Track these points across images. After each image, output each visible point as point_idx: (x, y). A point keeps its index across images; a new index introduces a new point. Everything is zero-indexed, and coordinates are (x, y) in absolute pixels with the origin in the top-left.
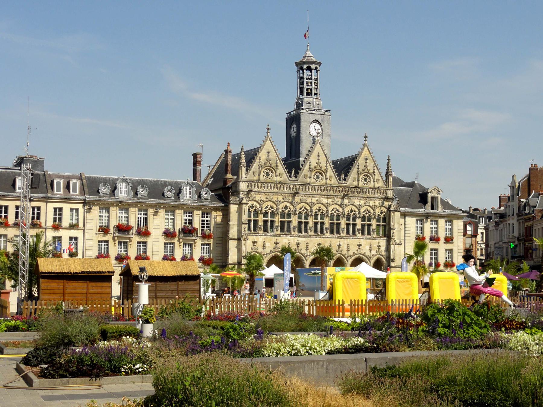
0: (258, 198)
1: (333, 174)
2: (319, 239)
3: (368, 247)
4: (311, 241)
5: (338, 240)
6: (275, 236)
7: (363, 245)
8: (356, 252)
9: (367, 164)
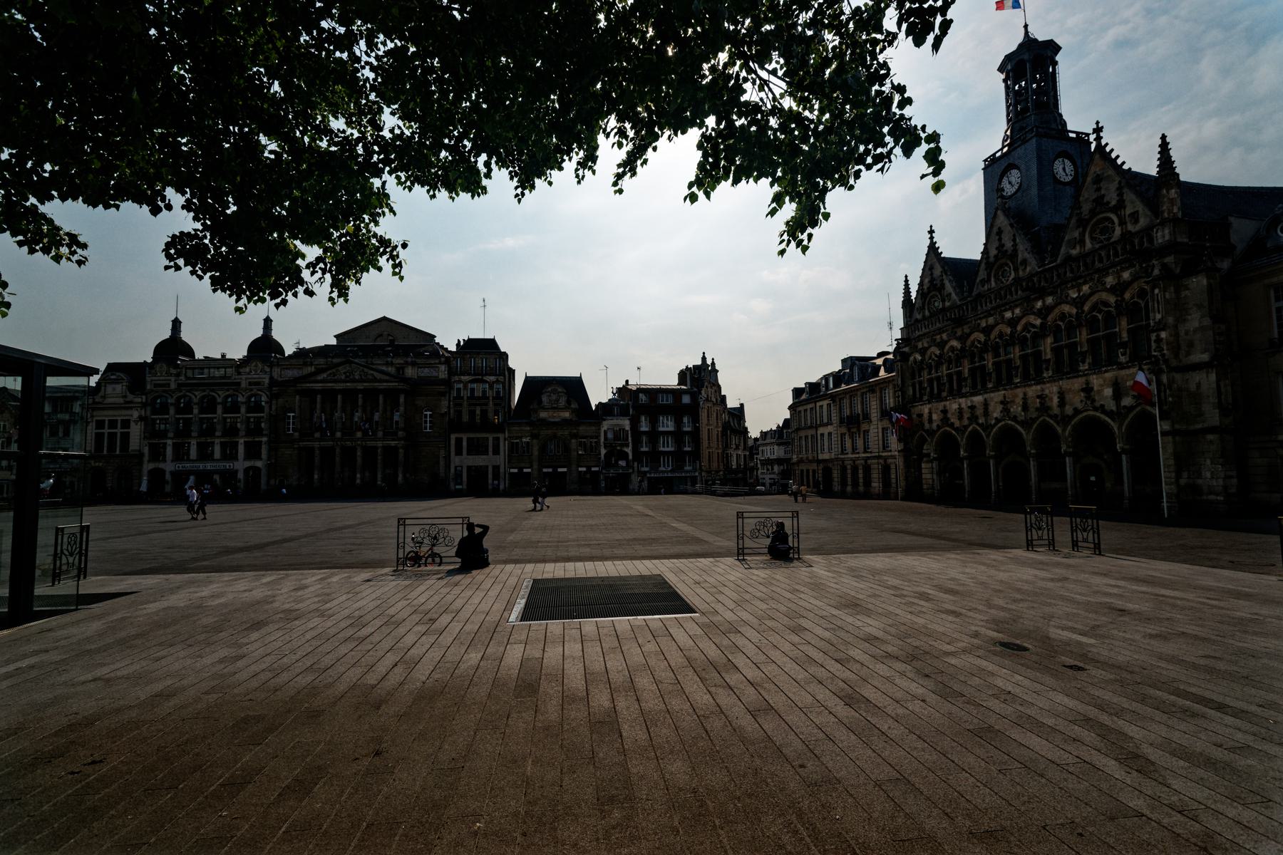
0: (920, 345)
1: (1027, 255)
2: (1003, 392)
3: (1108, 392)
4: (992, 399)
5: (1039, 387)
6: (941, 401)
7: (1095, 388)
8: (1080, 406)
9: (1103, 192)
